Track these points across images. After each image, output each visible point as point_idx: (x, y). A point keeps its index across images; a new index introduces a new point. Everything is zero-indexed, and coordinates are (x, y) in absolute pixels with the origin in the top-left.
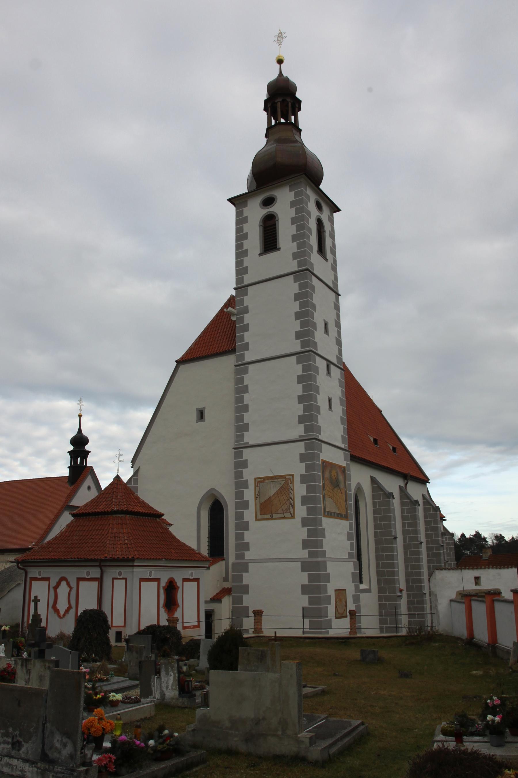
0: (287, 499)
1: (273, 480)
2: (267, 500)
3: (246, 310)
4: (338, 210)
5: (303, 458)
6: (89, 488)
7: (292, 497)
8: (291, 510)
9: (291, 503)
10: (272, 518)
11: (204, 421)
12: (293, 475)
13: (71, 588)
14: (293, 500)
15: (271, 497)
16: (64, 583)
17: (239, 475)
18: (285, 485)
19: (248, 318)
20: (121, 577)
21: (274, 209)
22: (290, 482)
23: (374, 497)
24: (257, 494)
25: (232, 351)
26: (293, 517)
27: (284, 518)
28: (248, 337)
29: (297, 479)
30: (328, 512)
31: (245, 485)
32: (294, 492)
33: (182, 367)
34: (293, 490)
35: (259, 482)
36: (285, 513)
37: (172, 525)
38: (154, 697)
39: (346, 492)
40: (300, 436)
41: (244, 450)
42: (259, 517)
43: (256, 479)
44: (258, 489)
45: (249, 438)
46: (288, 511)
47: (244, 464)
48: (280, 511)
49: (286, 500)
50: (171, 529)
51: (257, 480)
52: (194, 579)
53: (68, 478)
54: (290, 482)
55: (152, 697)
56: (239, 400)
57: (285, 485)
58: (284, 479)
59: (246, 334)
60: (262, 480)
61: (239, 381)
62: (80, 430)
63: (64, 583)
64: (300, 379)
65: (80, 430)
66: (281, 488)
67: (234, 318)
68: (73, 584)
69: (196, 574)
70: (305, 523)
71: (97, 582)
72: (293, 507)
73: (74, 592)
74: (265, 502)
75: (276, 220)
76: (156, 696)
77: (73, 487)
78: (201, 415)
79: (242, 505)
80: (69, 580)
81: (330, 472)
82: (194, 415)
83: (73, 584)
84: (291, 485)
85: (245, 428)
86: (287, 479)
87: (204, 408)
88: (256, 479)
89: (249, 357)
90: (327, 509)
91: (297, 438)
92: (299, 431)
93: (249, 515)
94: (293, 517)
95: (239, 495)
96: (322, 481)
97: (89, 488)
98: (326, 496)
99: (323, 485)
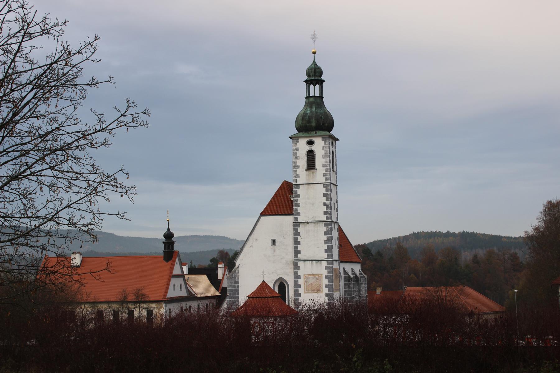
3: (298, 196)
4: (338, 140)
5: (326, 268)
6: (177, 263)
7: (321, 284)
8: (321, 290)
9: (321, 287)
11: (276, 245)
15: (311, 283)
17: (295, 273)
19: (300, 200)
21: (313, 148)
23: (345, 277)
25: (292, 214)
26: (322, 292)
28: (300, 209)
31: (299, 277)
33: (263, 218)
40: (325, 259)
42: (306, 291)
43: (304, 275)
51: (305, 276)
53: (163, 257)
61: (295, 230)
62: (169, 229)
64: (326, 233)
65: (169, 229)
67: (292, 199)
70: (327, 295)
72: (322, 288)
75: (315, 154)
77: (170, 262)
78: (274, 242)
79: (297, 286)
82: (270, 242)
84: (321, 279)
85: (299, 252)
88: (304, 275)
89: (300, 219)
92: (325, 256)
93: (301, 291)
94: (322, 292)
95: (296, 282)
97: (177, 263)
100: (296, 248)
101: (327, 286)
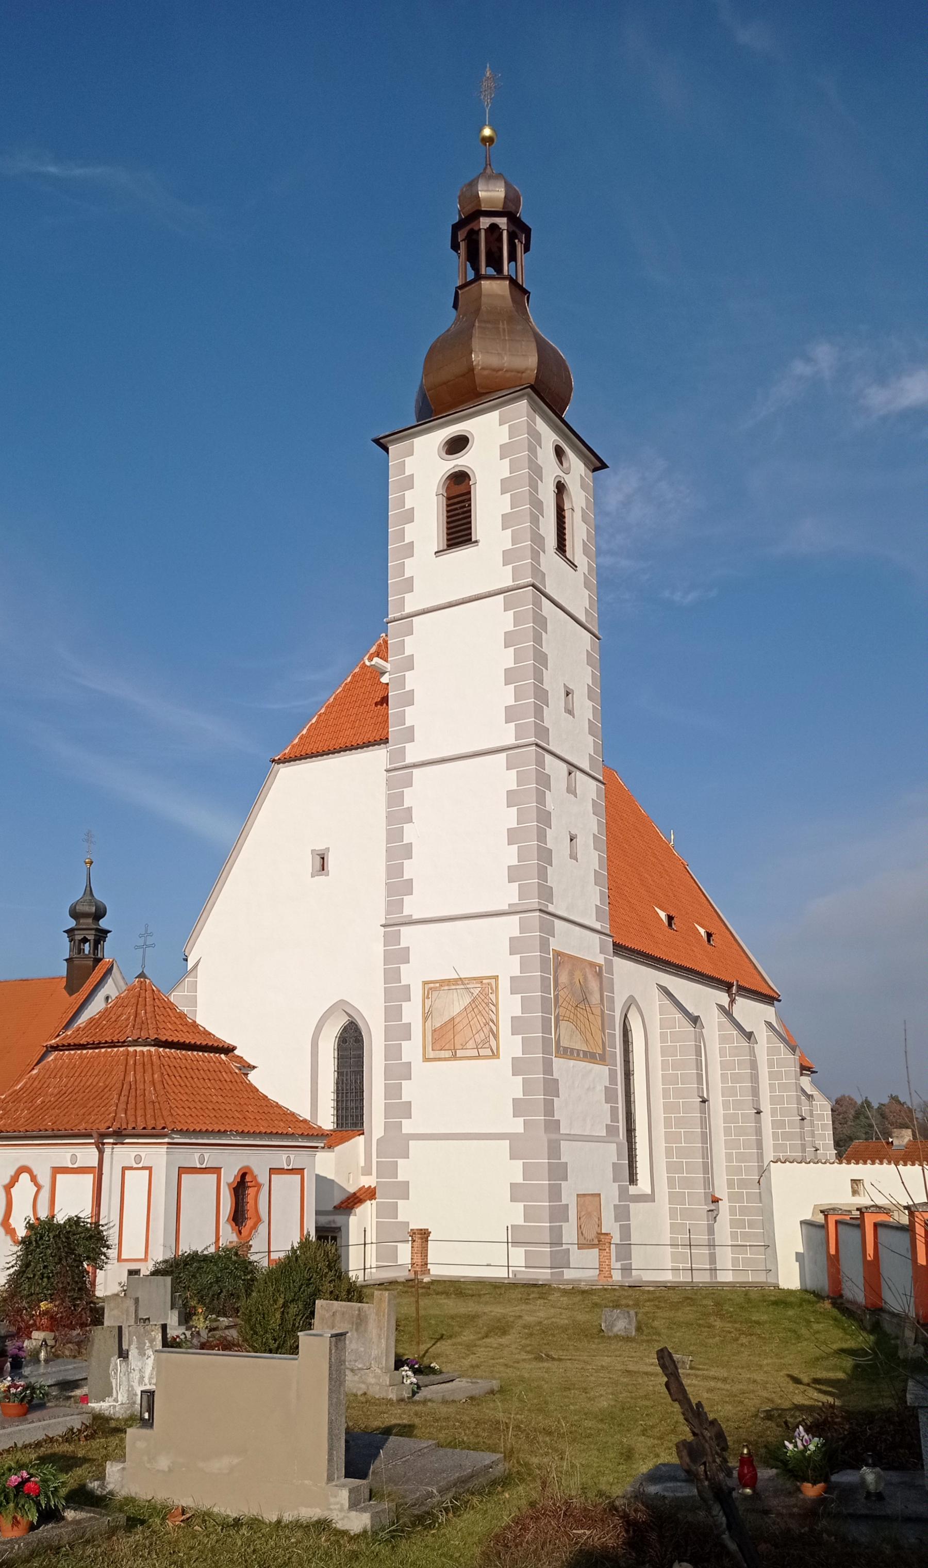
0: (485, 1021)
1: (457, 987)
2: (446, 1024)
7: (494, 1017)
8: (493, 1043)
10: (454, 1057)
12: (496, 978)
13: (39, 1187)
14: (497, 1026)
15: (453, 1018)
16: (25, 1177)
17: (392, 976)
18: (481, 996)
20: (140, 1165)
22: (490, 991)
24: (426, 1012)
26: (495, 1055)
27: (479, 1057)
29: (504, 985)
30: (565, 1049)
32: (497, 1010)
34: (496, 1005)
35: (432, 988)
36: (481, 1048)
37: (254, 1067)
38: (116, 1400)
39: (602, 1012)
41: (403, 929)
44: (428, 1002)
45: (412, 907)
46: (487, 1045)
47: (404, 956)
48: (471, 1044)
49: (482, 1025)
50: (253, 1078)
52: (292, 1169)
54: (490, 991)
55: (111, 1399)
56: (394, 835)
57: (481, 996)
58: (479, 985)
59: (409, 710)
60: (438, 985)
63: (25, 1177)
66: (473, 1001)
68: (44, 1179)
69: (296, 1159)
70: (518, 1067)
71: (91, 1176)
72: (496, 1037)
73: (45, 1195)
74: (441, 1027)
76: (120, 1399)
78: (322, 863)
80: (35, 1173)
81: (571, 974)
82: (308, 863)
83: (44, 1179)
84: (493, 997)
86: (485, 984)
87: (328, 849)
90: (564, 1043)
91: (505, 907)
94: (495, 1055)
96: (554, 991)
98: (561, 1018)
99: (556, 997)
100: (394, 871)
101: (517, 1026)
